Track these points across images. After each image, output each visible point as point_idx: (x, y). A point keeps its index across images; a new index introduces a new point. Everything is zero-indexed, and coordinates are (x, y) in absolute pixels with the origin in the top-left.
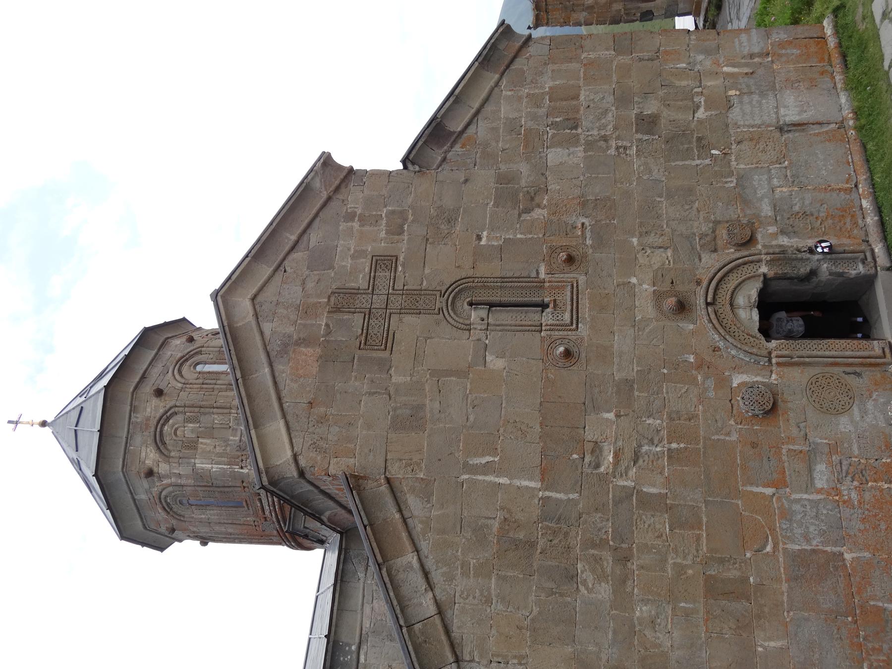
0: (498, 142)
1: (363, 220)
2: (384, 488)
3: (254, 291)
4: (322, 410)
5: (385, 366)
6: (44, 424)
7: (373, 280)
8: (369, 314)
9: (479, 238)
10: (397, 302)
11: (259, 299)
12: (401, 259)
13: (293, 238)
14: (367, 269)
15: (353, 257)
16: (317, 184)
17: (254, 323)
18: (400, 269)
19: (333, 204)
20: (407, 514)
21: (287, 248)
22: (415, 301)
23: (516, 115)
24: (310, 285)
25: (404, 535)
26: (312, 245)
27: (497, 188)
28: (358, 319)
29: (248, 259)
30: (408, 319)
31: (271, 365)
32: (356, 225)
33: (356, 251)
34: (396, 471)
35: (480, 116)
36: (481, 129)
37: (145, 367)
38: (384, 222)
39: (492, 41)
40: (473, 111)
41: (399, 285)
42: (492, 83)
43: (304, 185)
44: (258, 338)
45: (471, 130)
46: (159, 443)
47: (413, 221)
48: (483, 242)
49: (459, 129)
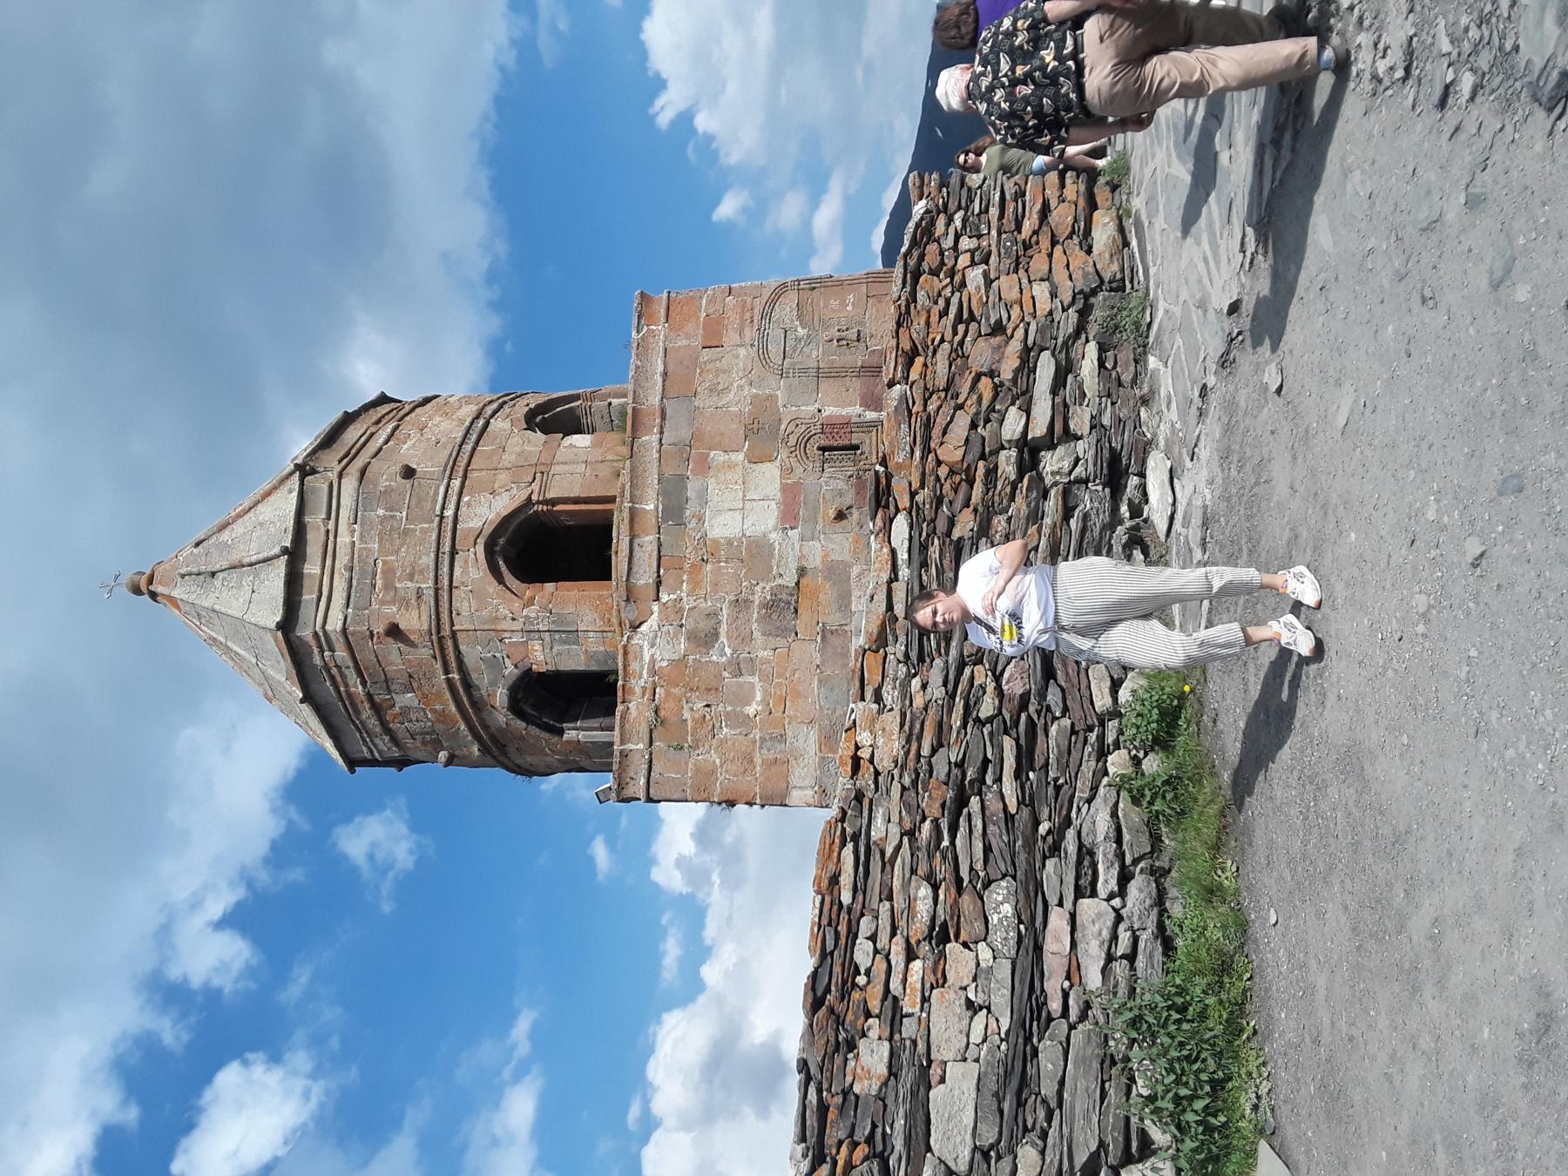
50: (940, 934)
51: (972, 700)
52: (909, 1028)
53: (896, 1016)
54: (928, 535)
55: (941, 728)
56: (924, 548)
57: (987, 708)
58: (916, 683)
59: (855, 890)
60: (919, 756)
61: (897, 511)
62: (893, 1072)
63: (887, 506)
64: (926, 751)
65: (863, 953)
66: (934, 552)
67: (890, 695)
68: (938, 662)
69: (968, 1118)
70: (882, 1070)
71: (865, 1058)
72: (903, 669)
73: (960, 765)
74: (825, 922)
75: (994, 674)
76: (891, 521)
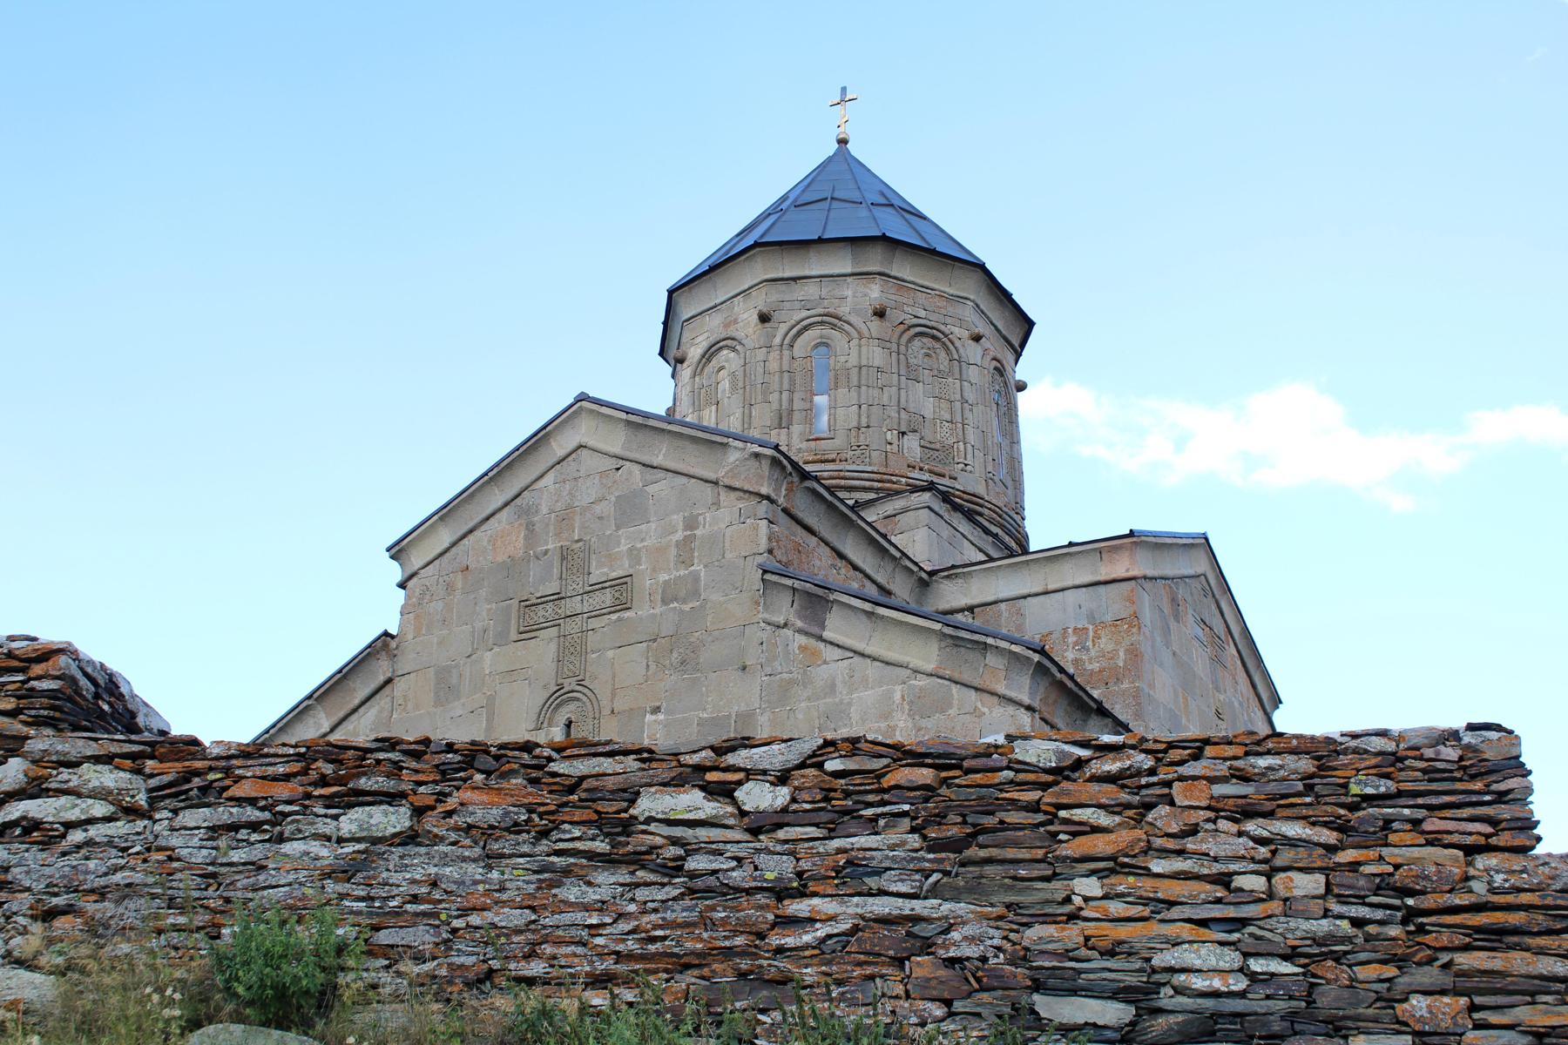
0: (809, 699)
1: (688, 540)
2: (382, 679)
3: (591, 443)
4: (459, 585)
5: (501, 640)
6: (843, 142)
7: (601, 586)
8: (558, 597)
9: (656, 710)
10: (572, 627)
11: (585, 452)
12: (627, 614)
13: (658, 460)
14: (614, 575)
15: (630, 550)
16: (733, 457)
17: (555, 460)
18: (614, 617)
19: (708, 488)
20: (362, 710)
21: (646, 459)
22: (572, 650)
23: (855, 716)
24: (598, 509)
25: (341, 714)
26: (651, 489)
27: (729, 716)
28: (552, 587)
29: (623, 416)
30: (553, 647)
31: (506, 505)
32: (679, 535)
33: (639, 550)
34: (400, 686)
35: (857, 659)
36: (834, 667)
37: (813, 273)
38: (682, 573)
39: (990, 641)
40: (860, 646)
41: (593, 623)
42: (916, 662)
43: (725, 440)
44: (533, 477)
45: (831, 653)
46: (709, 354)
47: (682, 611)
48: (649, 718)
49: (827, 634)
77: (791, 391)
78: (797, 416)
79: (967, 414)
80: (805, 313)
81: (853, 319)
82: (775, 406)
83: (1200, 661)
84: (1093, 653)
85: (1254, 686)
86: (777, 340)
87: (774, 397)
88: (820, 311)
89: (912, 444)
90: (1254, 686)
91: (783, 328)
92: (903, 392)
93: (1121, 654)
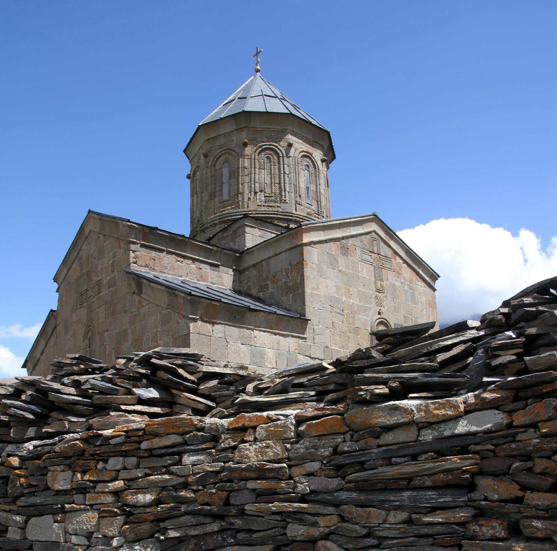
1: (114, 262)
50: (129, 513)
51: (298, 516)
52: (79, 498)
53: (82, 490)
54: (477, 452)
55: (270, 495)
56: (464, 450)
57: (296, 531)
58: (316, 466)
59: (150, 450)
60: (247, 480)
61: (510, 413)
62: (58, 493)
63: (516, 399)
64: (251, 485)
65: (115, 463)
66: (455, 461)
67: (301, 448)
68: (335, 483)
69: (41, 538)
70: (58, 486)
71: (61, 476)
72: (326, 452)
73: (242, 513)
74: (130, 434)
75: (331, 533)
76: (498, 409)
77: (215, 184)
78: (217, 194)
79: (287, 179)
80: (220, 150)
81: (236, 149)
82: (210, 191)
83: (366, 272)
84: (290, 278)
85: (417, 273)
86: (210, 164)
87: (209, 187)
88: (225, 148)
89: (261, 197)
90: (417, 273)
91: (212, 158)
92: (257, 176)
93: (299, 277)
